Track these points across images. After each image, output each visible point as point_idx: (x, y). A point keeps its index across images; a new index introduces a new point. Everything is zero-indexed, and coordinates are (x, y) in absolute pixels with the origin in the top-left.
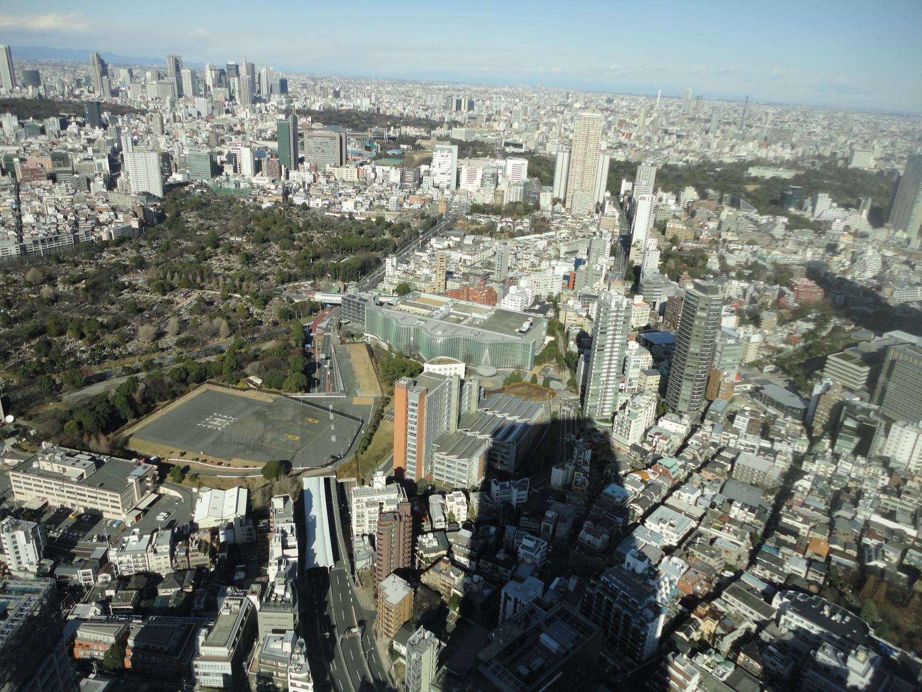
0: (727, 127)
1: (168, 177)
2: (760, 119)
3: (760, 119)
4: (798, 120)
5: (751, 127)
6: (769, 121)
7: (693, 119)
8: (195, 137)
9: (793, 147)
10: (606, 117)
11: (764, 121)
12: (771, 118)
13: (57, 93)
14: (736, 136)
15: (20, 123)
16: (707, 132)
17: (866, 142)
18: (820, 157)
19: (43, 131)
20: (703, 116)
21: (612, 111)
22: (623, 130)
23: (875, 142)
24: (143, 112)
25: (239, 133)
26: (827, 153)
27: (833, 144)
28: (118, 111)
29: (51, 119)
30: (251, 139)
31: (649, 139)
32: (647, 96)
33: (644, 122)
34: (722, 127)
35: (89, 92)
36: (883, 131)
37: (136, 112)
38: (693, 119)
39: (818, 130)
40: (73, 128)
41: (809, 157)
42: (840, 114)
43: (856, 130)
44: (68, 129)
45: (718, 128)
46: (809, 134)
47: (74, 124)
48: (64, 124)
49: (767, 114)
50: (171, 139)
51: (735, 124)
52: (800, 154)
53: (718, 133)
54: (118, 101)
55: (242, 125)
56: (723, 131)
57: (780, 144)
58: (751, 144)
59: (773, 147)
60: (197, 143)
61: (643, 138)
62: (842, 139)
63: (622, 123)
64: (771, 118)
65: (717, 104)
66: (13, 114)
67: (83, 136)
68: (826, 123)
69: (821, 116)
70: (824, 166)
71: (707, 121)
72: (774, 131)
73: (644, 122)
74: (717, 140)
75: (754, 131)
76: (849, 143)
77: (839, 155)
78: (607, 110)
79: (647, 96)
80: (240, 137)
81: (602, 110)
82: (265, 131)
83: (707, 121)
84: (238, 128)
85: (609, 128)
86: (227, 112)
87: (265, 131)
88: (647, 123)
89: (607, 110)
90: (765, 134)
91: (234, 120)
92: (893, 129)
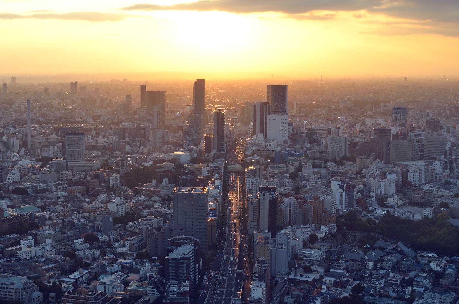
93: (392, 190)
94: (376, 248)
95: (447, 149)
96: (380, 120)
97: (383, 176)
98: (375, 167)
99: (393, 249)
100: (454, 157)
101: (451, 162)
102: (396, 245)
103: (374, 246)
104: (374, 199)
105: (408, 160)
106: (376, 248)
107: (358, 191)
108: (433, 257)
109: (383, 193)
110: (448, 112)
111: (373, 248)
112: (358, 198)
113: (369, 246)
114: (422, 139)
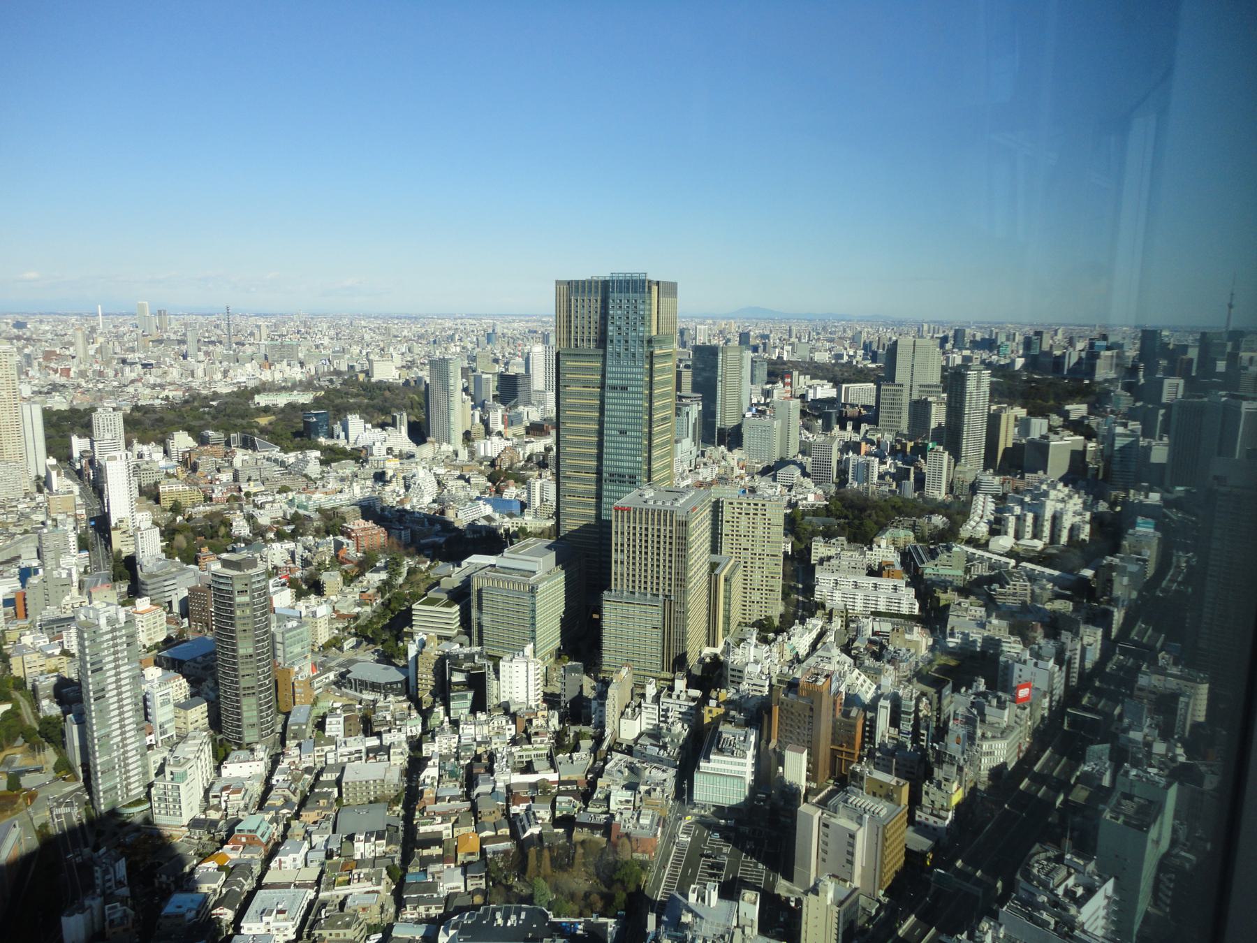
0: (211, 348)
2: (252, 334)
3: (252, 334)
4: (298, 332)
5: (243, 345)
6: (264, 336)
7: (160, 342)
9: (302, 364)
10: (20, 350)
11: (257, 336)
12: (265, 331)
14: (227, 358)
16: (185, 357)
17: (382, 350)
18: (338, 373)
20: (173, 337)
21: (27, 339)
22: (53, 365)
23: (391, 349)
26: (344, 368)
27: (347, 356)
31: (101, 374)
32: (80, 315)
33: (86, 351)
34: (204, 348)
36: (396, 337)
38: (160, 342)
39: (326, 341)
41: (324, 374)
42: (345, 321)
43: (367, 337)
45: (199, 350)
46: (317, 347)
49: (259, 327)
51: (221, 343)
52: (313, 372)
53: (201, 356)
56: (207, 353)
57: (285, 362)
58: (248, 365)
59: (278, 366)
61: (90, 374)
62: (355, 349)
63: (48, 355)
64: (265, 331)
65: (188, 319)
68: (332, 332)
69: (325, 326)
70: (345, 383)
71: (182, 342)
72: (273, 347)
73: (86, 351)
74: (202, 366)
75: (249, 350)
76: (364, 353)
77: (358, 368)
78: (18, 338)
79: (80, 315)
81: (10, 339)
83: (182, 342)
85: (30, 365)
88: (92, 352)
89: (18, 338)
90: (263, 351)
92: (405, 333)
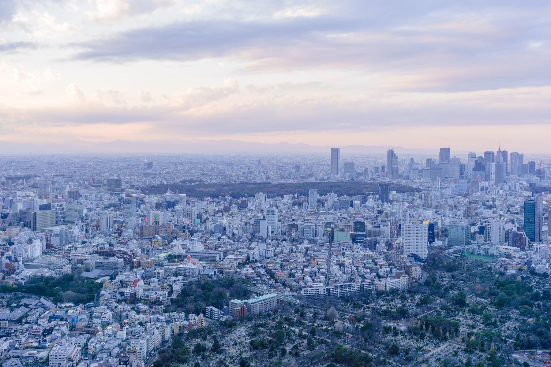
1: (431, 242)
8: (455, 210)
13: (362, 177)
15: (338, 200)
19: (351, 205)
24: (418, 190)
25: (490, 207)
28: (401, 190)
29: (357, 196)
30: (501, 213)
35: (383, 176)
37: (413, 190)
40: (370, 202)
44: (367, 203)
47: (371, 200)
48: (364, 200)
50: (436, 212)
54: (403, 182)
55: (494, 200)
60: (456, 216)
66: (335, 193)
67: (376, 208)
80: (491, 211)
82: (512, 206)
84: (491, 203)
86: (482, 189)
87: (512, 206)
91: (487, 197)
93: (38, 252)
94: (21, 305)
95: (84, 215)
96: (29, 192)
97: (30, 241)
98: (25, 233)
99: (36, 305)
100: (89, 221)
101: (87, 225)
102: (39, 301)
103: (20, 304)
104: (21, 263)
105: (52, 226)
106: (21, 305)
107: (7, 257)
108: (70, 307)
109: (29, 256)
110: (87, 183)
111: (19, 306)
112: (7, 264)
113: (15, 305)
114: (63, 208)
